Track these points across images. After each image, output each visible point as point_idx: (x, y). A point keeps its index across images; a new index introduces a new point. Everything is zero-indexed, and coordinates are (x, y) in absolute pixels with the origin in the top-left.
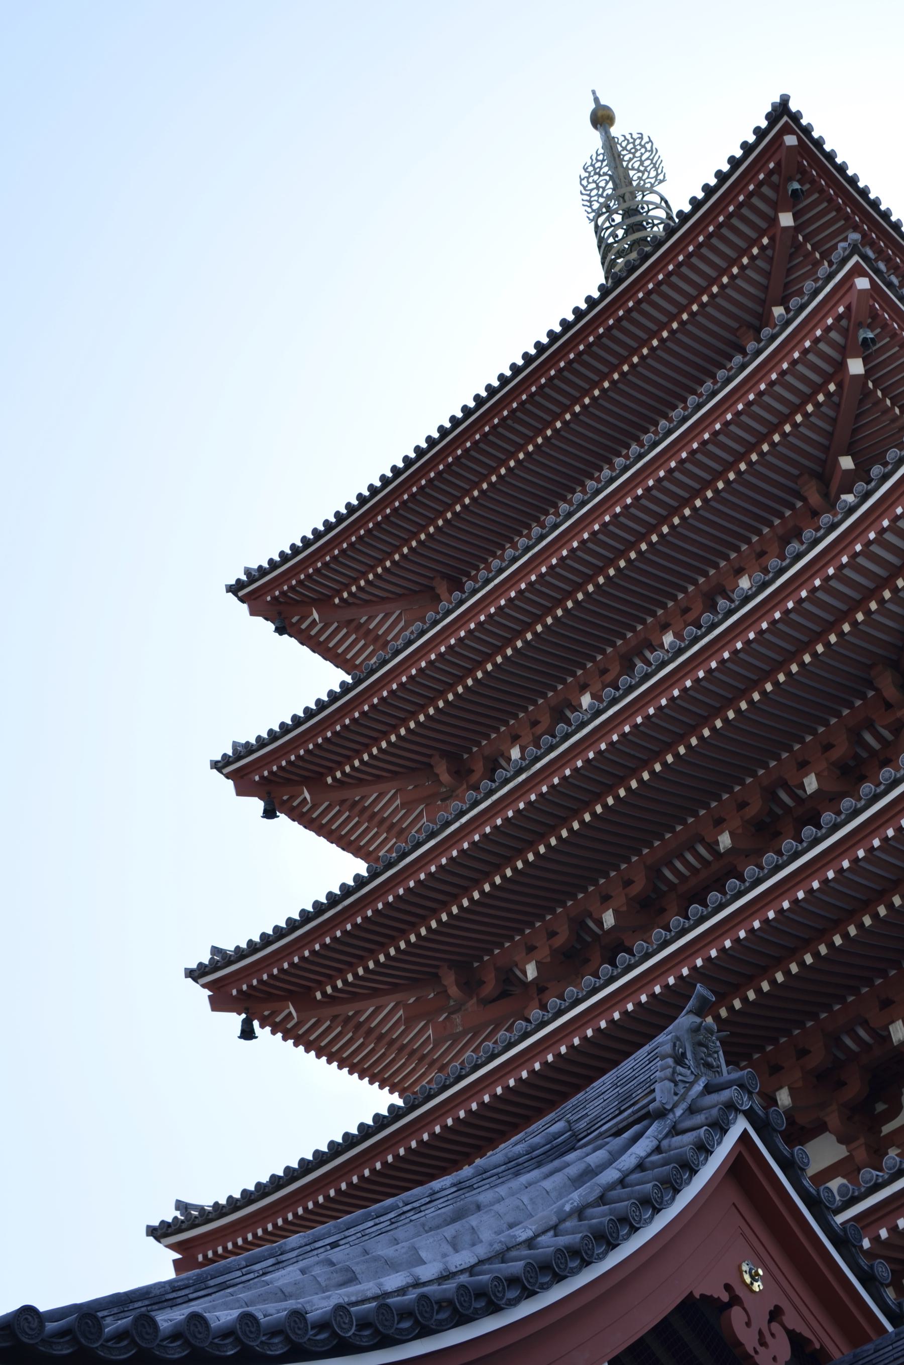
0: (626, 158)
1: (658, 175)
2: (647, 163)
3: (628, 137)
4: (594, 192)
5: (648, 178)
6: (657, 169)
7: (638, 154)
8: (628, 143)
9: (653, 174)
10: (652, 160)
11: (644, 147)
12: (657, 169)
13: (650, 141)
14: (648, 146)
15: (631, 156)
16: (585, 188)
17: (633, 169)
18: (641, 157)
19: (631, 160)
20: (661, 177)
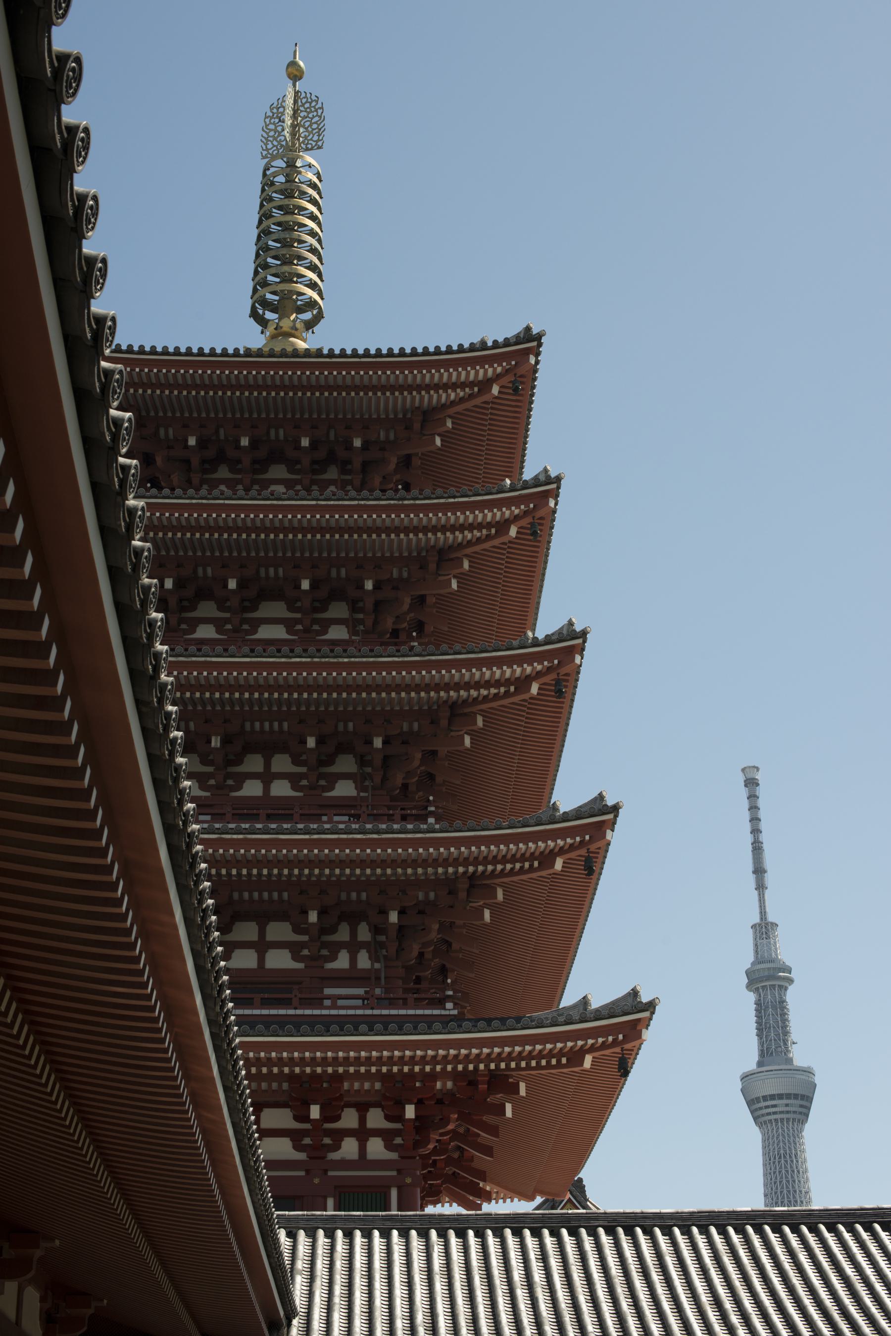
0: (302, 114)
1: (318, 140)
2: (315, 126)
3: (308, 95)
4: (272, 133)
5: (311, 139)
6: (319, 136)
7: (310, 115)
8: (306, 102)
9: (316, 138)
10: (319, 125)
11: (316, 110)
12: (319, 136)
13: (322, 108)
14: (320, 111)
15: (305, 114)
16: (267, 125)
17: (304, 126)
18: (312, 119)
19: (305, 117)
20: (320, 143)
